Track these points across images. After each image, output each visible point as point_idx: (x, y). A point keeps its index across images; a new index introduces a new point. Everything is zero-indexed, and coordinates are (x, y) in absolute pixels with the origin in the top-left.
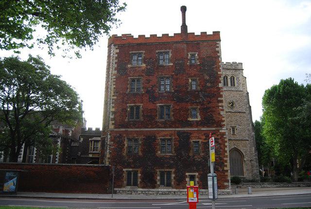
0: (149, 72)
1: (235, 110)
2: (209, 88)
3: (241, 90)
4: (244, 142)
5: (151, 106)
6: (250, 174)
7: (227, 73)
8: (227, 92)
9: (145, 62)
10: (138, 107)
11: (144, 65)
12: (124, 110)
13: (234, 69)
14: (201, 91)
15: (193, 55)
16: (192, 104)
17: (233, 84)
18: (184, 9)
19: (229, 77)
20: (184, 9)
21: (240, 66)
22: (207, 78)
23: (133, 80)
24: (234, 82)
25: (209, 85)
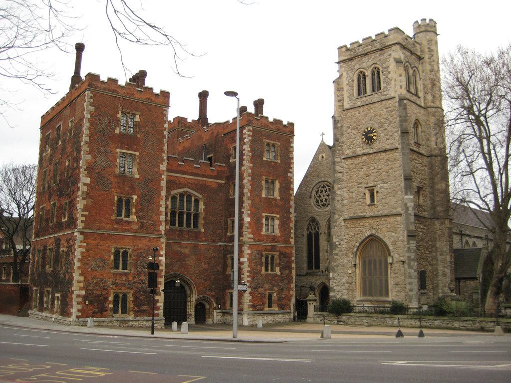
1: (377, 146)
3: (393, 95)
4: (392, 219)
6: (403, 294)
7: (364, 65)
8: (361, 109)
13: (377, 50)
17: (376, 87)
18: (80, 48)
19: (368, 73)
20: (80, 48)
24: (379, 82)
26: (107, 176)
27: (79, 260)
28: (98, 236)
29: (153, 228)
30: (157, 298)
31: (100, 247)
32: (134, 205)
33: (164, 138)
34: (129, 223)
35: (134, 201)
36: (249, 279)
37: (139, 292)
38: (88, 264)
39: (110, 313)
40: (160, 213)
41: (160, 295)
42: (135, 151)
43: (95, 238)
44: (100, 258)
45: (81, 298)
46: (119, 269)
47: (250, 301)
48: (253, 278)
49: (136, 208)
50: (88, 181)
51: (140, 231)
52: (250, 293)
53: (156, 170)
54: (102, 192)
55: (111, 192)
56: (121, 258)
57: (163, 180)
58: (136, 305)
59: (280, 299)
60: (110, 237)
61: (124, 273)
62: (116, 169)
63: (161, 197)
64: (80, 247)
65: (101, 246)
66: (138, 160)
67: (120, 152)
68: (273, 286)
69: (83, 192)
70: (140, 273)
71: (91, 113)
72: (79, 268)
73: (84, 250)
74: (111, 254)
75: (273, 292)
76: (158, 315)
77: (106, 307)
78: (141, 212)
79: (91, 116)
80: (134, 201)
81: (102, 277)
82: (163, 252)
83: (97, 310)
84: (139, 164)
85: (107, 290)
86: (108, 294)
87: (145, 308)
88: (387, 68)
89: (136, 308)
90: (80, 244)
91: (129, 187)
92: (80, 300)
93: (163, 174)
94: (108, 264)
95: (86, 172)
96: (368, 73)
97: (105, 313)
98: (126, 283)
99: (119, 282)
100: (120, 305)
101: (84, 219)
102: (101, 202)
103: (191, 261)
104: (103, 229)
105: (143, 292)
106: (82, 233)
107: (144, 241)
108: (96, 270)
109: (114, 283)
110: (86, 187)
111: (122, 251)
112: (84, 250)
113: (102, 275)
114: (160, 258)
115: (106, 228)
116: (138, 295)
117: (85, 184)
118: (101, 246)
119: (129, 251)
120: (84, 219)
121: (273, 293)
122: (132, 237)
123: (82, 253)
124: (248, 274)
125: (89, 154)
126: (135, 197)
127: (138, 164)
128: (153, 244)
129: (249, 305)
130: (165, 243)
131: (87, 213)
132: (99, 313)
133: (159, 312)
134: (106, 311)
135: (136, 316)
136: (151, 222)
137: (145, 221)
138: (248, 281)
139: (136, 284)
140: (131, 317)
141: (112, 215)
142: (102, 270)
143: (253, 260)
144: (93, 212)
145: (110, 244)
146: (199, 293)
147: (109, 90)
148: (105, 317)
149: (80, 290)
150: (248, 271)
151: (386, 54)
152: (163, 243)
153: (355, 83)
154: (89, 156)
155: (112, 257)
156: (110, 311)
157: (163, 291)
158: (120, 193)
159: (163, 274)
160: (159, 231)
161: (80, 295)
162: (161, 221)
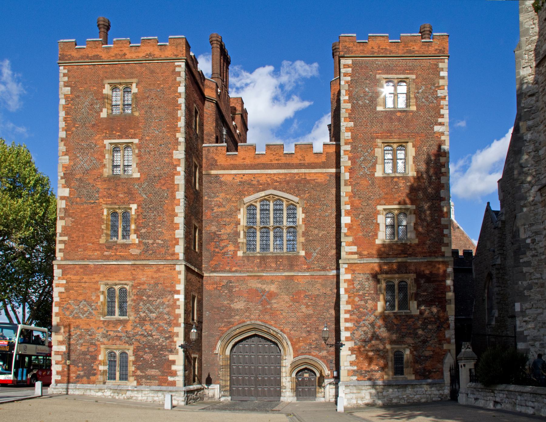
26: (91, 181)
27: (58, 304)
28: (81, 268)
29: (163, 250)
30: (171, 357)
31: (83, 285)
32: (132, 218)
33: (178, 110)
34: (126, 246)
35: (133, 212)
36: (349, 325)
37: (145, 348)
38: (68, 308)
39: (100, 378)
40: (175, 227)
41: (177, 353)
42: (132, 138)
43: (77, 272)
44: (85, 300)
45: (60, 356)
46: (114, 315)
47: (352, 364)
48: (357, 323)
49: (135, 223)
50: (65, 192)
51: (143, 257)
52: (352, 350)
53: (167, 160)
54: (85, 206)
55: (99, 204)
56: (117, 300)
57: (179, 173)
58: (138, 368)
59: (417, 359)
60: (98, 269)
61: (121, 322)
62: (105, 170)
63: (176, 202)
64: (58, 286)
65: (86, 282)
66: (137, 151)
67: (111, 144)
68: (403, 337)
69: (60, 209)
70: (145, 320)
71: (66, 97)
72: (57, 314)
73: (62, 290)
74: (99, 294)
75: (403, 346)
76: (173, 384)
77: (95, 370)
78: (144, 227)
79: (66, 102)
80: (133, 212)
81: (88, 327)
82: (181, 287)
83: (82, 373)
84: (139, 156)
85: (95, 345)
86: (98, 351)
87: (153, 372)
89: (139, 373)
90: (57, 282)
91: (125, 193)
92: (59, 358)
93: (179, 165)
94: (96, 308)
95: (63, 181)
97: (92, 378)
98: (123, 334)
99: (112, 333)
100: (118, 368)
101: (62, 246)
102: (84, 221)
103: (281, 303)
104: (89, 259)
105: (149, 348)
106: (60, 267)
107: (149, 272)
108: (79, 317)
109: (105, 336)
110: (64, 202)
111: (117, 288)
112: (62, 290)
113: (88, 324)
114: (176, 296)
115: (93, 257)
116: (141, 354)
117: (62, 198)
118: (86, 282)
119: (128, 287)
120: (62, 246)
121: (404, 349)
122: (129, 267)
123: (60, 293)
124: (347, 316)
125: (66, 155)
126: (134, 207)
127: (138, 156)
128: (163, 274)
129: (348, 371)
130: (183, 273)
131: (66, 238)
132: (85, 378)
133: (176, 379)
134: (95, 374)
135: (139, 384)
136: (160, 242)
137: (151, 242)
138: (347, 329)
139: (138, 337)
140: (132, 383)
141: (100, 238)
142: (87, 317)
143: (358, 290)
144: (74, 235)
145: (97, 279)
146: (297, 352)
147: (88, 57)
148: (93, 384)
149: (58, 345)
150: (347, 312)
152: (179, 273)
154: (67, 157)
155: (102, 298)
156: (101, 375)
157: (182, 346)
158: (111, 204)
159: (181, 320)
160: (173, 254)
161: (58, 352)
162: (175, 239)
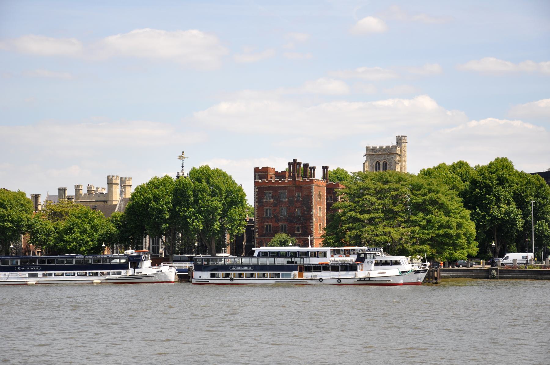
0: (275, 205)
2: (306, 214)
5: (276, 225)
9: (273, 198)
10: (270, 226)
11: (272, 200)
12: (263, 227)
14: (302, 216)
15: (298, 195)
16: (297, 224)
19: (381, 163)
21: (394, 149)
22: (305, 208)
23: (267, 209)
25: (306, 213)
88: (391, 163)
96: (381, 163)
151: (390, 157)
153: (375, 166)
